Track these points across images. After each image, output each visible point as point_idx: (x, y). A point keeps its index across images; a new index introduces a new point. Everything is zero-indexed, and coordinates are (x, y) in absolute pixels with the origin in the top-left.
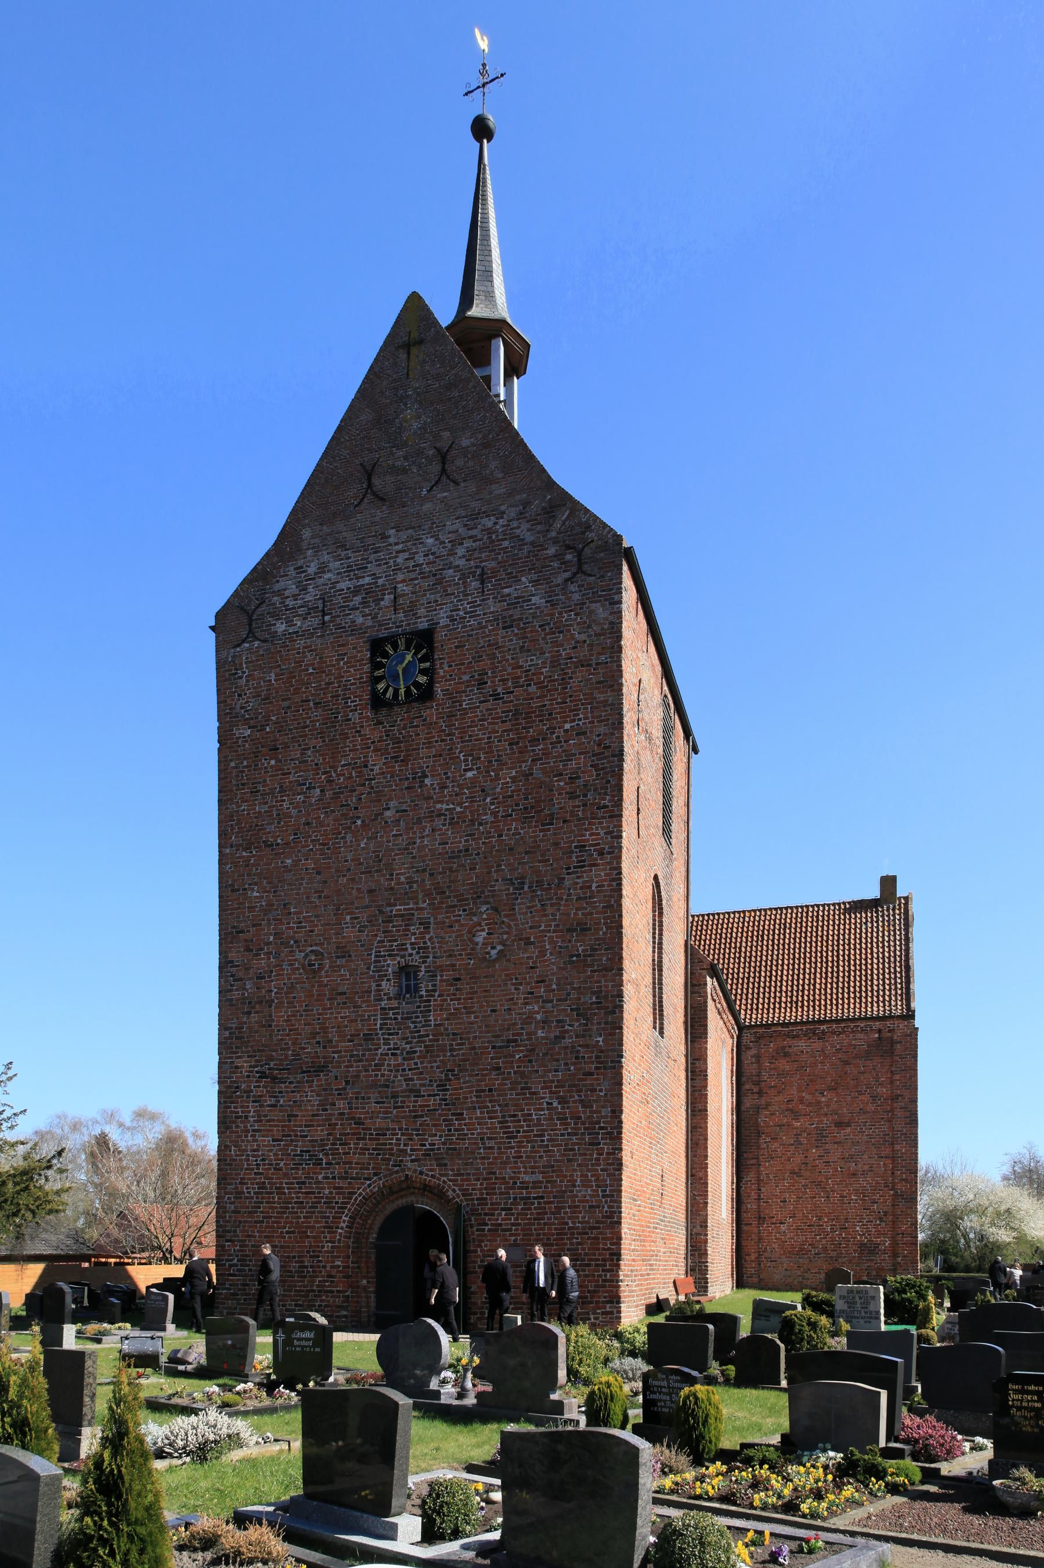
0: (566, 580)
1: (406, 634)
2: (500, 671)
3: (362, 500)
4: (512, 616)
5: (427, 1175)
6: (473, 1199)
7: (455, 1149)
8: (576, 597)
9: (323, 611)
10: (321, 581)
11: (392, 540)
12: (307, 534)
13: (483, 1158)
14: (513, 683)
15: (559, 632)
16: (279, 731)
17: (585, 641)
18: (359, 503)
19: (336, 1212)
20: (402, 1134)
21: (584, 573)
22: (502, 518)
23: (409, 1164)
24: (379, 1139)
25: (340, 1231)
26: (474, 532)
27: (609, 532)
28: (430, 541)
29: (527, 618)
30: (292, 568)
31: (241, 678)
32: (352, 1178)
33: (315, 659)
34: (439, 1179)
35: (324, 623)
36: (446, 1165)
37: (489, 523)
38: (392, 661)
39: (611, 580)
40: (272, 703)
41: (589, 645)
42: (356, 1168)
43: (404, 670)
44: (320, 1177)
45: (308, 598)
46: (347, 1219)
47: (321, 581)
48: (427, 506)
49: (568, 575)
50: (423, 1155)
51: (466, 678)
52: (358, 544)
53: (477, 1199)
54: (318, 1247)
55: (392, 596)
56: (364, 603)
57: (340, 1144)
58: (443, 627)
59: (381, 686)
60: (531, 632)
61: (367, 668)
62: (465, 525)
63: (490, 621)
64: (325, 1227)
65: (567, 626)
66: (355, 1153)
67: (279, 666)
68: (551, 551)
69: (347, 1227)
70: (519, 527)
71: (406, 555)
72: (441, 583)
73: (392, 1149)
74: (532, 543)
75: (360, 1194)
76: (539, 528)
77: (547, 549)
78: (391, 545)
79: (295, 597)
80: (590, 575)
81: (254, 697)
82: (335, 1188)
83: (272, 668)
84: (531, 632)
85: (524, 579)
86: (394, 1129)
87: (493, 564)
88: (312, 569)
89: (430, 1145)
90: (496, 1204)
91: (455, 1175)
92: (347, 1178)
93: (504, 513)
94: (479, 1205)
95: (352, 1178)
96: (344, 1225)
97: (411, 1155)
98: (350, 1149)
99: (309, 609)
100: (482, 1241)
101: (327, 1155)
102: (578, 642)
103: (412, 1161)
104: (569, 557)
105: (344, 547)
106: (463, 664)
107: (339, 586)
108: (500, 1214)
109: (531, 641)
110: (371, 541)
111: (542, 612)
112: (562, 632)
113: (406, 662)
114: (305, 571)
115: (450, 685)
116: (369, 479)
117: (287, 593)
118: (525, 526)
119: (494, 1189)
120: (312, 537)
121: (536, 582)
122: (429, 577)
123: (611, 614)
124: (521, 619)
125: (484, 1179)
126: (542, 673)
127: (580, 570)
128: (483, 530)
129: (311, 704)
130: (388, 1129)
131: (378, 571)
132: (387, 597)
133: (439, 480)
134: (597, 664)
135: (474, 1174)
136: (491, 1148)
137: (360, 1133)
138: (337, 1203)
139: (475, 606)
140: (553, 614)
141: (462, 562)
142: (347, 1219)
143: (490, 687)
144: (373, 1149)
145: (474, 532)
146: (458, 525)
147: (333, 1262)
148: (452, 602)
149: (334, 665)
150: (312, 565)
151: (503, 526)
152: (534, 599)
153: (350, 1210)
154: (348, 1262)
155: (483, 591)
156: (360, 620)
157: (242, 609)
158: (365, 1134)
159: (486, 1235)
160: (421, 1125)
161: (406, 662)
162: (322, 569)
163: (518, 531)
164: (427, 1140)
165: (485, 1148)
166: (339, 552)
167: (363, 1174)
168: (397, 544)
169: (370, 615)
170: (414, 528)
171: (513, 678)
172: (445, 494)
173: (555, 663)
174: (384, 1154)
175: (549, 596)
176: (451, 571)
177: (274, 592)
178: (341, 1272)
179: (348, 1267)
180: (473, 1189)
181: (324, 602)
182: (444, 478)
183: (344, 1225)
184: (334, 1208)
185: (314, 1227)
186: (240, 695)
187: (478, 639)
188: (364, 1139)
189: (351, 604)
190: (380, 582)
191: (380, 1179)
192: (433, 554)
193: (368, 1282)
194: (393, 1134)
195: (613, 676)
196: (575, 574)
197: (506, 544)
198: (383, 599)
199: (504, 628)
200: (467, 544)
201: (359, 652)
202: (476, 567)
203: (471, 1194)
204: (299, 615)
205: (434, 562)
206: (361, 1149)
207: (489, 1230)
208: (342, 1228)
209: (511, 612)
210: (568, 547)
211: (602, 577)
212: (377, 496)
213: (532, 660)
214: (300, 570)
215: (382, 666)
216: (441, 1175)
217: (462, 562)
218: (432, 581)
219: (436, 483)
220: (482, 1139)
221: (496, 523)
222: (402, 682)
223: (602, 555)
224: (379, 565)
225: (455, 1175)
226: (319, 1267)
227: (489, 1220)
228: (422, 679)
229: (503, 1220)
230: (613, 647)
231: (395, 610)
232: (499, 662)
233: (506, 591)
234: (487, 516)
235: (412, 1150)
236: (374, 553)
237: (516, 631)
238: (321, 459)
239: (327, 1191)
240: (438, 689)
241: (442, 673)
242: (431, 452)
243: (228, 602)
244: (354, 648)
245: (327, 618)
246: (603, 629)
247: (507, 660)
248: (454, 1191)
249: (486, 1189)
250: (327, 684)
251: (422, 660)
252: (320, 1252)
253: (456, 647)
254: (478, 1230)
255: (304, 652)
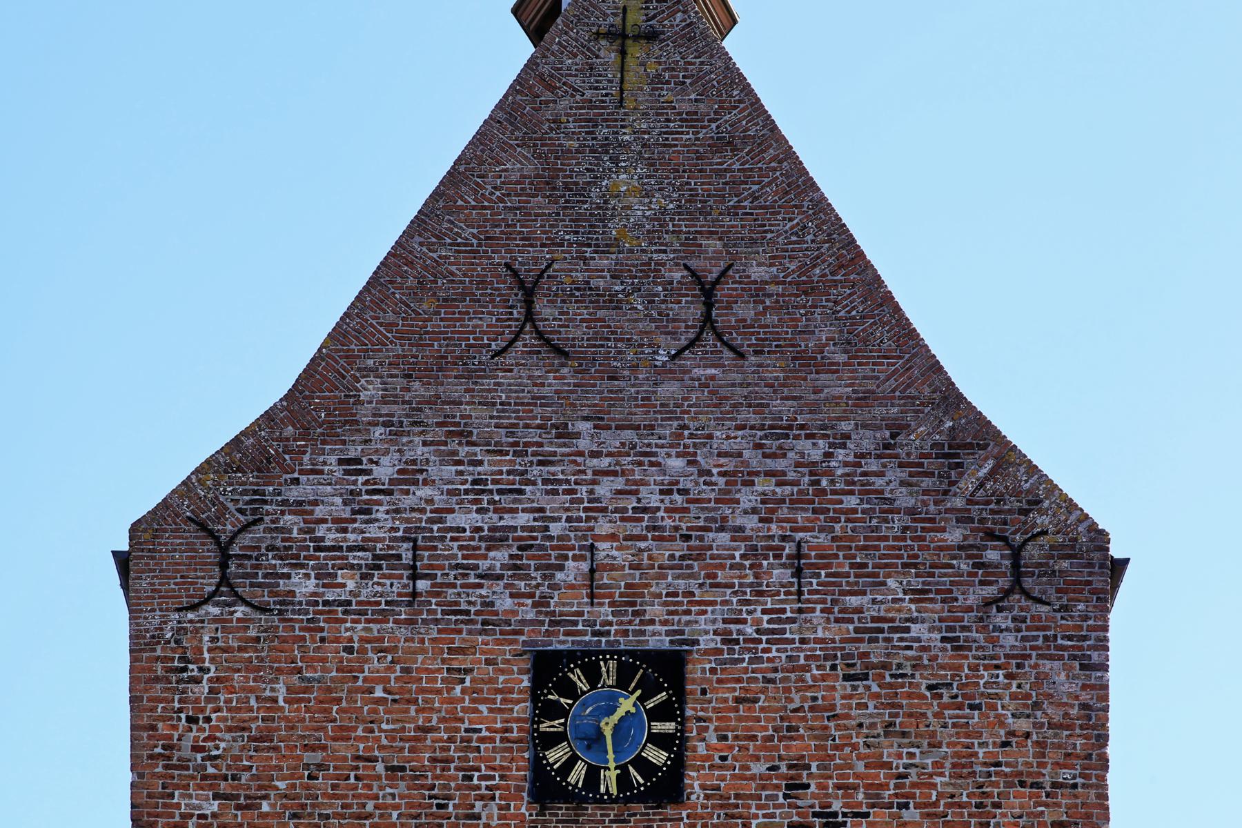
0: (987, 603)
1: (620, 653)
2: (838, 767)
3: (511, 343)
4: (865, 655)
8: (1009, 640)
9: (414, 567)
10: (407, 502)
11: (584, 444)
12: (371, 390)
14: (867, 796)
15: (972, 707)
16: (294, 816)
17: (1028, 735)
18: (504, 350)
21: (1027, 595)
22: (844, 446)
26: (780, 464)
27: (1080, 521)
28: (677, 464)
29: (899, 666)
30: (333, 459)
31: (197, 681)
33: (389, 669)
35: (414, 594)
37: (816, 452)
38: (585, 705)
39: (1086, 618)
40: (276, 749)
41: (1037, 743)
43: (616, 728)
45: (373, 532)
47: (407, 502)
48: (669, 389)
49: (990, 591)
51: (759, 768)
52: (501, 436)
55: (585, 566)
56: (516, 567)
58: (707, 652)
59: (556, 755)
60: (910, 696)
61: (522, 709)
62: (758, 446)
63: (817, 658)
65: (989, 696)
67: (299, 671)
68: (954, 536)
70: (880, 474)
71: (619, 483)
72: (699, 557)
74: (911, 512)
76: (926, 483)
77: (943, 530)
78: (581, 454)
79: (341, 525)
80: (1039, 601)
81: (229, 729)
83: (279, 670)
84: (910, 696)
85: (891, 583)
87: (823, 539)
88: (385, 471)
93: (847, 437)
99: (375, 557)
102: (1012, 733)
104: (992, 555)
105: (464, 435)
106: (754, 738)
107: (451, 520)
109: (910, 715)
110: (533, 436)
111: (933, 659)
112: (977, 707)
113: (620, 712)
114: (367, 472)
115: (723, 778)
116: (529, 304)
117: (319, 512)
118: (895, 474)
120: (384, 401)
121: (919, 595)
122: (672, 539)
123: (1084, 687)
124: (885, 666)
126: (934, 786)
127: (1017, 585)
128: (798, 465)
129: (380, 767)
131: (551, 505)
132: (570, 564)
133: (698, 337)
134: (1055, 785)
139: (779, 621)
140: (960, 667)
141: (751, 523)
143: (814, 796)
145: (780, 464)
146: (740, 442)
148: (724, 603)
149: (438, 692)
150: (385, 460)
151: (846, 464)
152: (915, 629)
155: (800, 593)
156: (505, 603)
157: (202, 526)
161: (620, 712)
162: (410, 475)
163: (879, 482)
166: (453, 446)
168: (595, 454)
169: (532, 595)
170: (638, 428)
171: (868, 786)
172: (712, 371)
173: (962, 769)
175: (950, 629)
176: (724, 538)
177: (285, 502)
181: (415, 548)
182: (709, 337)
186: (190, 720)
187: (787, 690)
189: (484, 565)
190: (556, 529)
192: (681, 492)
195: (1088, 816)
196: (1007, 593)
197: (851, 502)
198: (561, 568)
199: (847, 678)
200: (764, 485)
201: (502, 672)
202: (784, 538)
204: (352, 567)
205: (686, 510)
209: (864, 647)
210: (991, 535)
211: (1065, 608)
212: (548, 342)
213: (911, 755)
214: (351, 465)
215: (563, 712)
217: (751, 523)
218: (680, 548)
219: (691, 344)
221: (828, 455)
222: (611, 756)
223: (1065, 564)
224: (555, 492)
228: (657, 756)
230: (1089, 757)
231: (592, 596)
232: (836, 748)
233: (854, 601)
234: (808, 437)
236: (540, 463)
237: (875, 689)
238: (408, 233)
240: (694, 782)
241: (701, 749)
242: (677, 276)
243: (165, 504)
244: (488, 662)
245: (422, 585)
246: (1066, 715)
247: (855, 747)
250: (418, 729)
251: (655, 715)
253: (738, 700)
255: (362, 651)
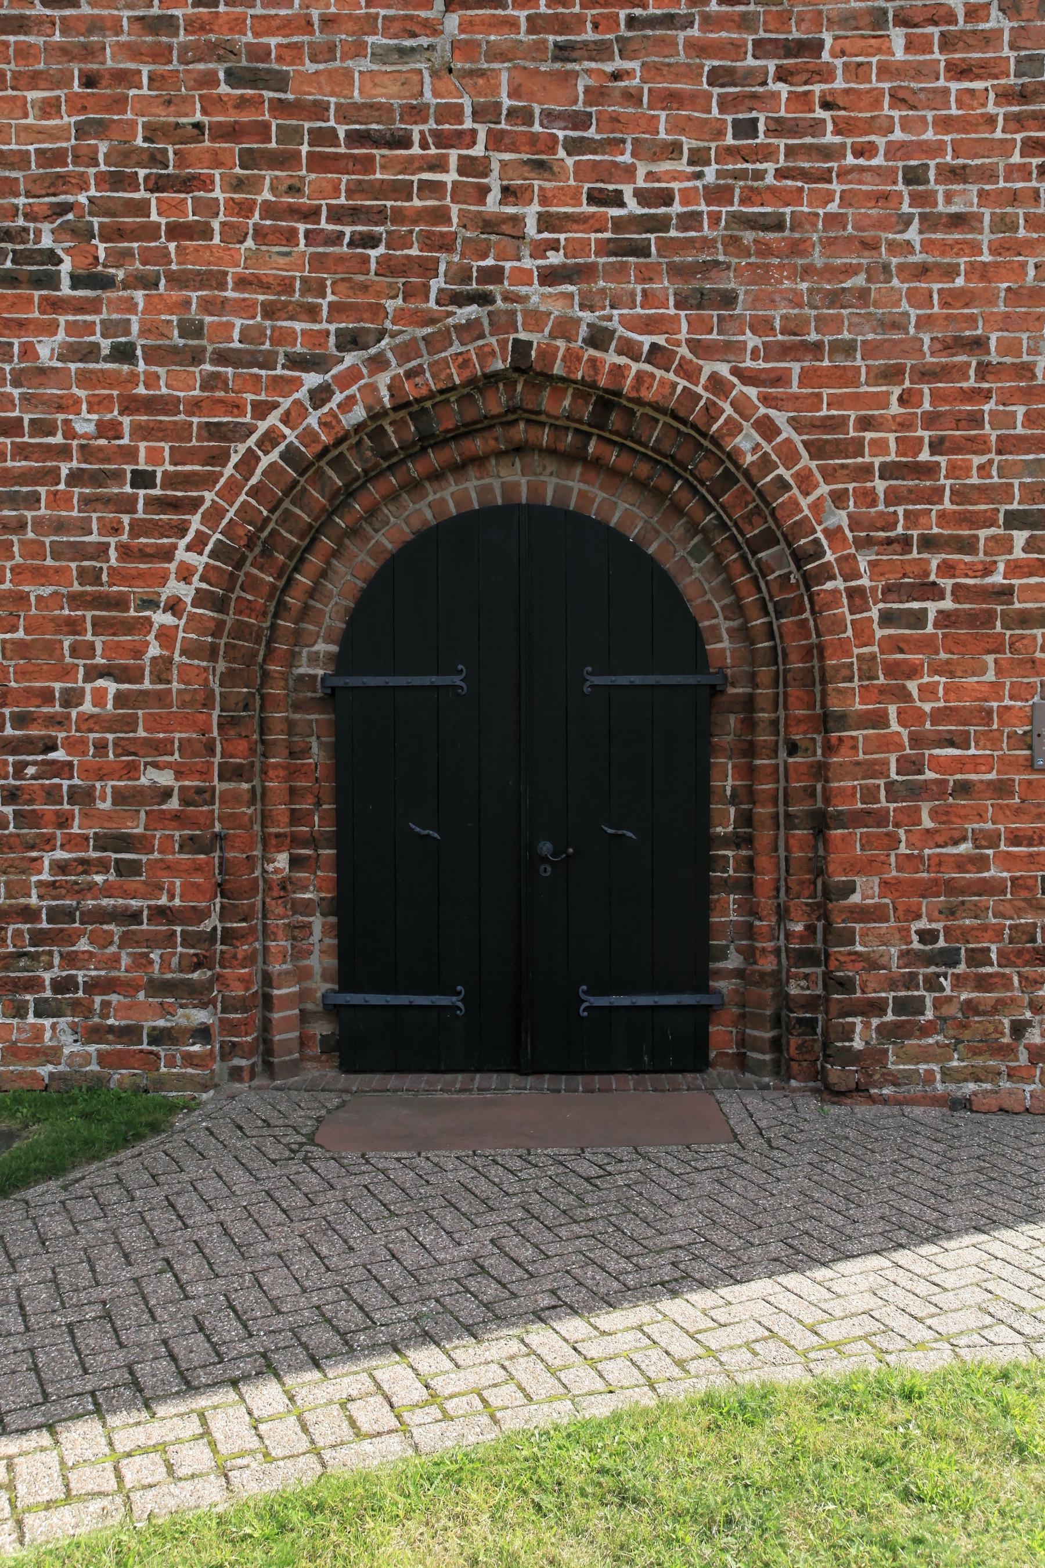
5: (629, 349)
6: (866, 471)
7: (778, 225)
13: (923, 271)
19: (138, 528)
20: (496, 141)
23: (535, 293)
24: (367, 164)
25: (161, 618)
32: (223, 358)
34: (689, 372)
36: (728, 299)
42: (245, 308)
44: (45, 350)
46: (199, 561)
50: (607, 248)
53: (888, 471)
54: (47, 696)
57: (157, 185)
64: (76, 600)
66: (234, 234)
69: (202, 596)
73: (441, 216)
75: (270, 440)
82: (131, 405)
86: (455, 113)
89: (642, 197)
90: (984, 492)
91: (772, 352)
92: (196, 357)
94: (893, 497)
95: (223, 358)
96: (186, 592)
97: (540, 249)
98: (211, 208)
100: (913, 672)
101: (82, 234)
103: (550, 276)
108: (1005, 544)
119: (975, 420)
125: (925, 374)
130: (417, 113)
135: (871, 350)
136: (958, 221)
137: (262, 131)
138: (143, 479)
142: (199, 561)
144: (337, 215)
147: (131, 771)
153: (214, 515)
154: (204, 773)
158: (290, 134)
159: (927, 645)
160: (595, 95)
164: (629, 172)
165: (929, 222)
167: (283, 337)
174: (396, 241)
178: (176, 817)
179: (205, 795)
180: (866, 423)
183: (186, 592)
184: (128, 505)
185: (24, 598)
188: (285, 160)
191: (378, 363)
193: (295, 862)
194: (443, 140)
203: (857, 447)
206: (268, 210)
207: (945, 619)
208: (174, 606)
216: (695, 346)
220: (914, 177)
225: (772, 352)
226: (52, 795)
227: (947, 569)
229: (1015, 569)
235: (546, 222)
239: (85, 424)
248: (767, 428)
249: (931, 420)
252: (60, 721)
254: (887, 618)
